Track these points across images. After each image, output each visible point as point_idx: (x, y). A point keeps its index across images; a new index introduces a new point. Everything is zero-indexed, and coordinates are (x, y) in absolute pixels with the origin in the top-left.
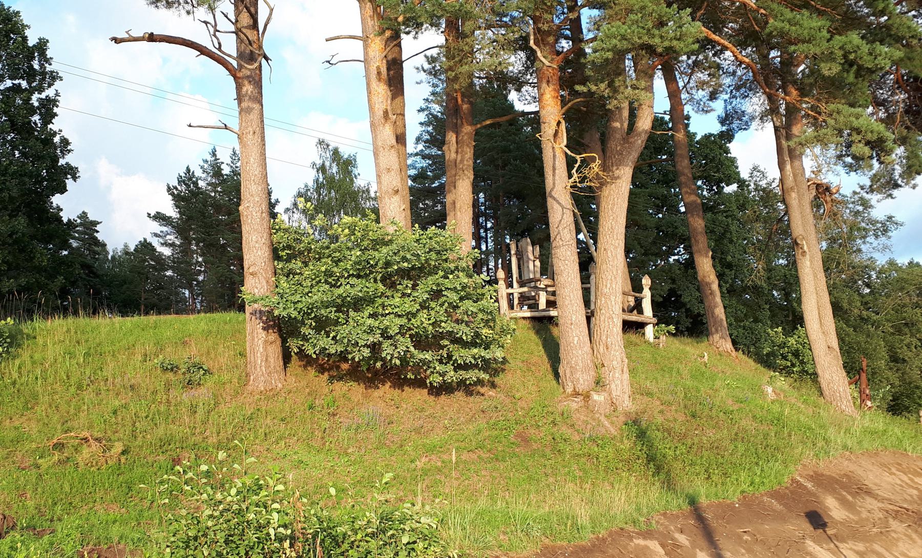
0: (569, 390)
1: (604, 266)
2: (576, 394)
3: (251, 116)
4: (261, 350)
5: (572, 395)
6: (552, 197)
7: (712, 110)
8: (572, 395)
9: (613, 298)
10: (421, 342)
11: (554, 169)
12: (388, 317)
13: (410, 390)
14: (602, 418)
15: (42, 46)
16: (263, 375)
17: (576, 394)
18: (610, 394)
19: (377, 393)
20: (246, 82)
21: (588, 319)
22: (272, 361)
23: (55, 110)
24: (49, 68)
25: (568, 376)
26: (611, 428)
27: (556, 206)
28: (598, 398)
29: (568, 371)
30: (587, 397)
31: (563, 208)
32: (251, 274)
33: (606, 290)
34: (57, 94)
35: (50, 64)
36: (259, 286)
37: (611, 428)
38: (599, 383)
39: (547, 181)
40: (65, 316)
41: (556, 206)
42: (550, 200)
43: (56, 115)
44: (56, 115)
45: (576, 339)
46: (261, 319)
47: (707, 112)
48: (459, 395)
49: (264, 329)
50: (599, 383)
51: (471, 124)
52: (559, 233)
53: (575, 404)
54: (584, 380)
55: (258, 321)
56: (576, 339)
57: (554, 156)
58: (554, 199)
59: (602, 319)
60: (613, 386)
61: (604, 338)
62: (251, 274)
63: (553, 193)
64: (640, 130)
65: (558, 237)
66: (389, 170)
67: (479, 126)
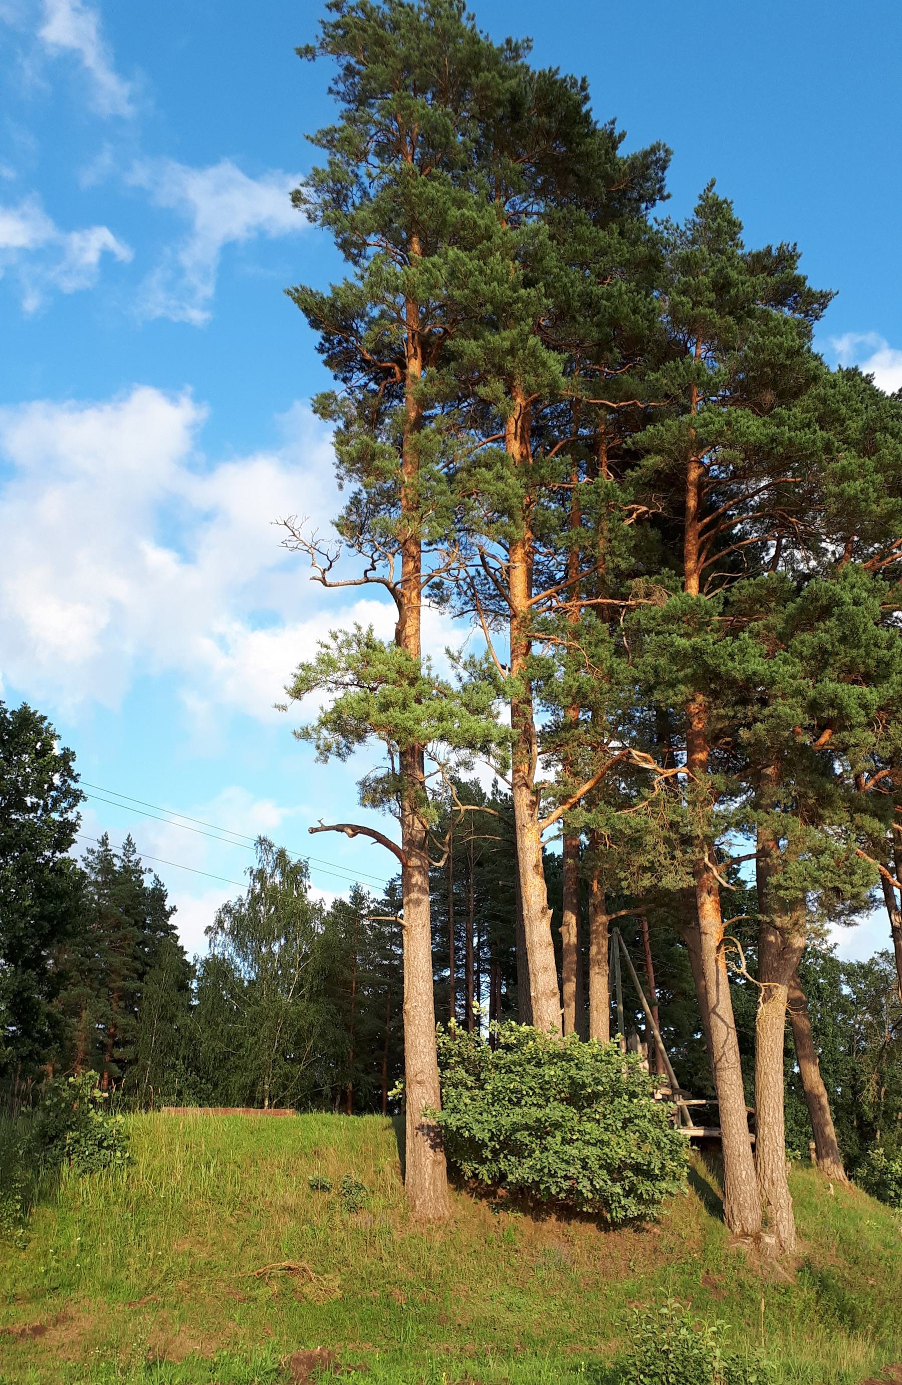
0: (738, 1230)
1: (766, 1092)
2: (745, 1235)
3: (421, 908)
4: (430, 1171)
5: (741, 1236)
6: (715, 1013)
7: (856, 924)
8: (741, 1236)
9: (776, 1128)
10: (615, 1171)
11: (718, 985)
12: (576, 1144)
13: (578, 1224)
14: (775, 1263)
15: (68, 756)
16: (430, 1200)
17: (745, 1235)
18: (779, 1236)
19: (546, 1226)
20: (416, 873)
21: (753, 1147)
22: (439, 1184)
23: (75, 836)
24: (74, 785)
25: (735, 1213)
26: (788, 1277)
27: (720, 1024)
28: (769, 1240)
29: (735, 1209)
30: (758, 1239)
31: (728, 1027)
32: (419, 1082)
33: (768, 1119)
34: (79, 817)
35: (76, 781)
36: (427, 1097)
37: (788, 1277)
38: (766, 1222)
39: (709, 996)
40: (147, 1111)
41: (720, 1024)
42: (713, 1017)
43: (74, 841)
44: (74, 841)
45: (744, 1173)
46: (428, 1135)
47: (849, 925)
48: (628, 1231)
49: (432, 1147)
50: (766, 1222)
51: (608, 913)
52: (724, 1054)
53: (746, 1246)
54: (752, 1220)
55: (426, 1138)
56: (744, 1173)
57: (718, 971)
58: (719, 1016)
59: (766, 1150)
60: (781, 1227)
61: (769, 1172)
62: (419, 1082)
63: (717, 1010)
64: (796, 946)
65: (724, 1059)
66: (546, 969)
67: (614, 916)
